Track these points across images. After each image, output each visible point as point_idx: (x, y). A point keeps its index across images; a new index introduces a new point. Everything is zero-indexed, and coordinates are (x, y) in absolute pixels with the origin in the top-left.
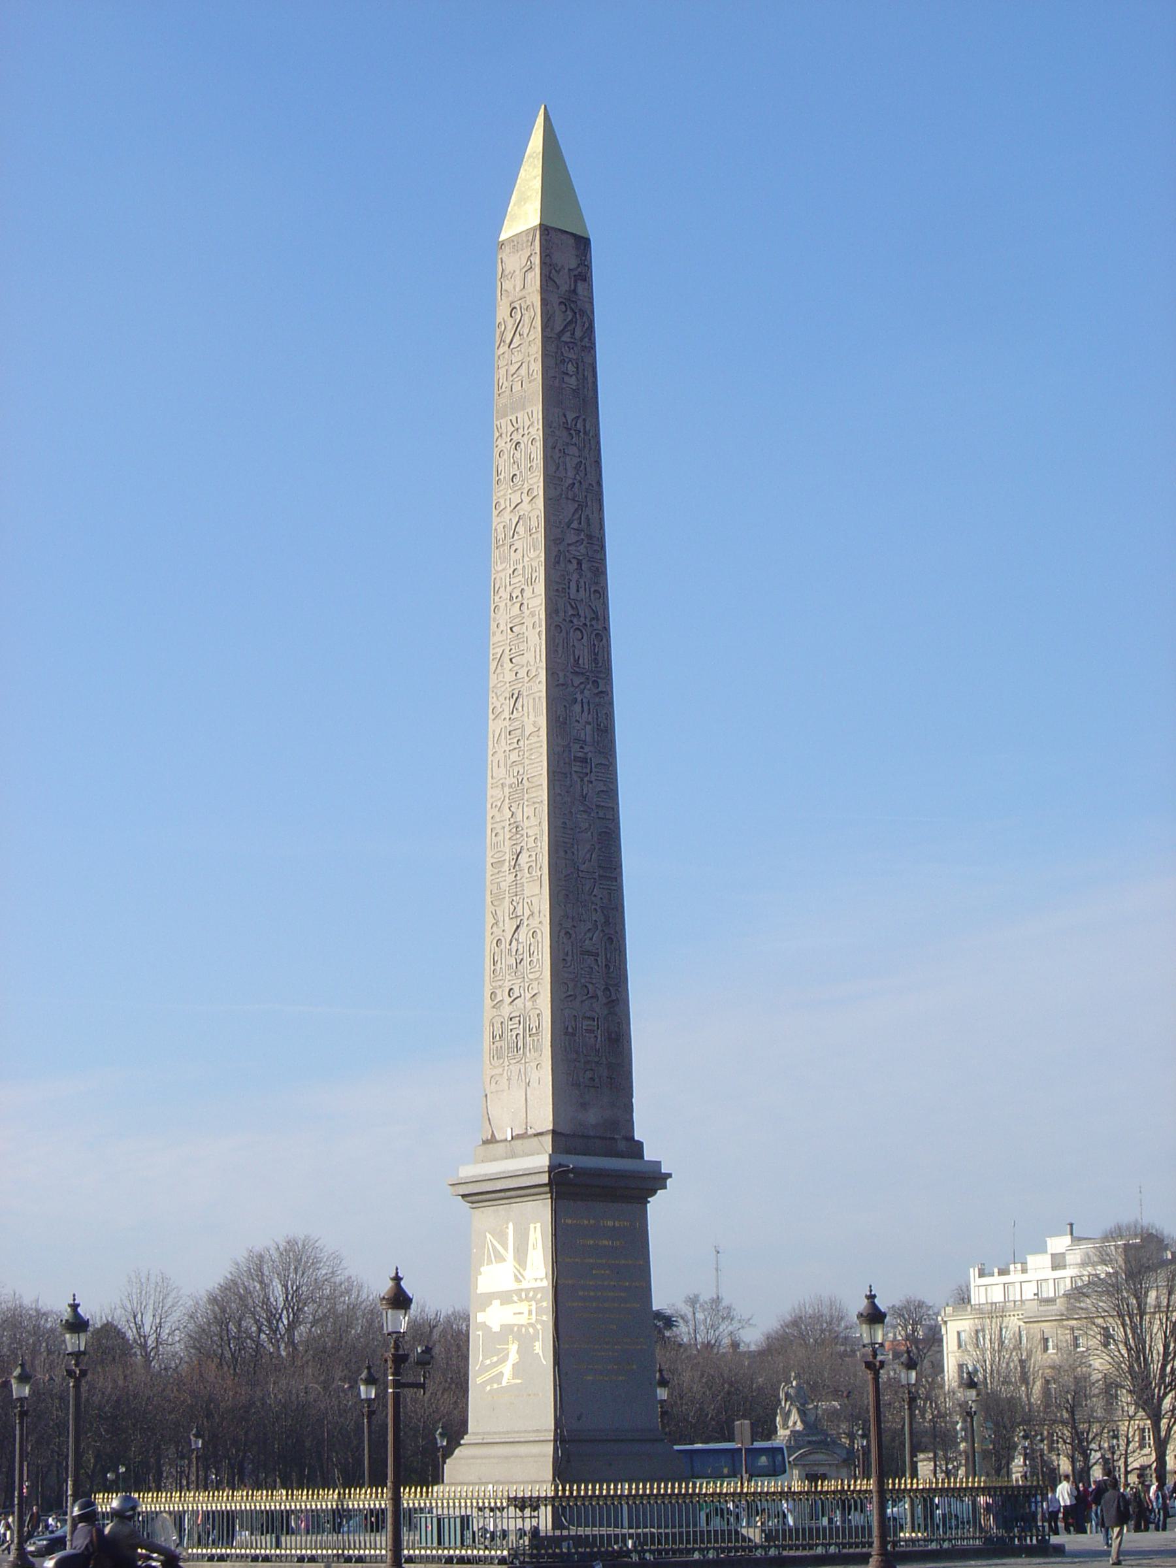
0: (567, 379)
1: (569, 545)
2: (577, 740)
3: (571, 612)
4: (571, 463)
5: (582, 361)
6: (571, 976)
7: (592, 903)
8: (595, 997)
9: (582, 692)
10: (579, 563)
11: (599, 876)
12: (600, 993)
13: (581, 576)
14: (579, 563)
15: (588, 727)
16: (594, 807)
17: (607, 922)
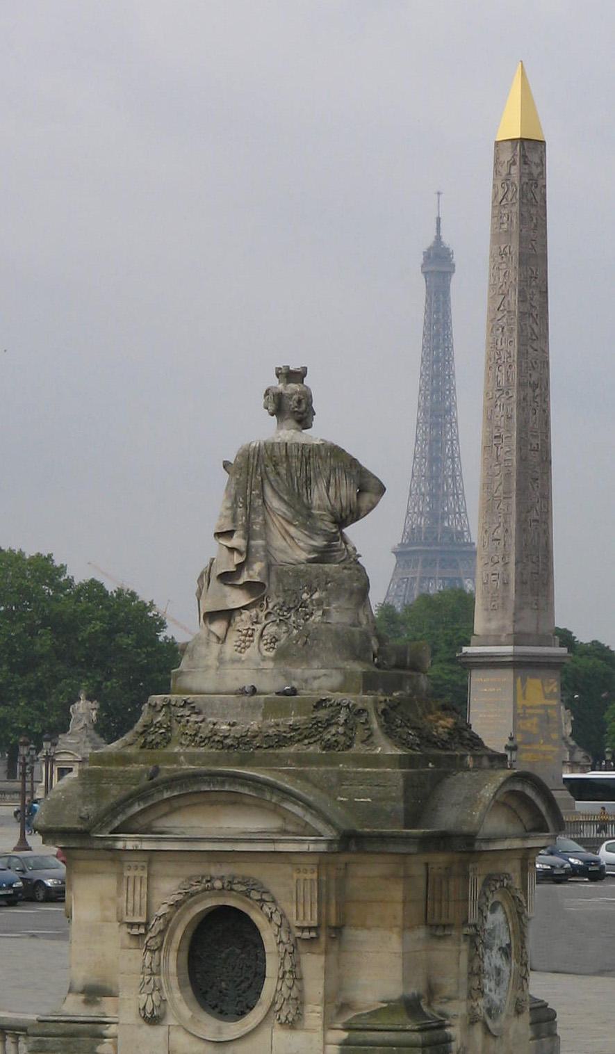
0: (503, 226)
1: (499, 320)
2: (496, 427)
3: (497, 357)
4: (501, 273)
5: (511, 212)
6: (486, 553)
7: (500, 513)
8: (498, 562)
9: (500, 400)
10: (503, 329)
11: (504, 498)
12: (500, 560)
13: (503, 335)
14: (503, 329)
15: (503, 418)
16: (503, 461)
17: (506, 522)
